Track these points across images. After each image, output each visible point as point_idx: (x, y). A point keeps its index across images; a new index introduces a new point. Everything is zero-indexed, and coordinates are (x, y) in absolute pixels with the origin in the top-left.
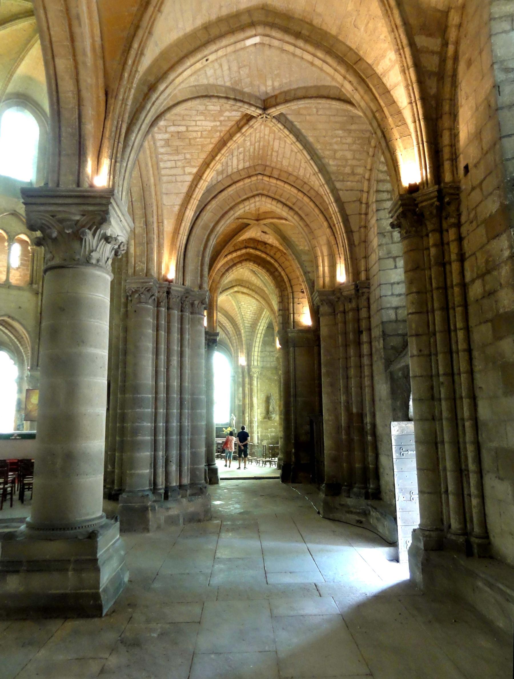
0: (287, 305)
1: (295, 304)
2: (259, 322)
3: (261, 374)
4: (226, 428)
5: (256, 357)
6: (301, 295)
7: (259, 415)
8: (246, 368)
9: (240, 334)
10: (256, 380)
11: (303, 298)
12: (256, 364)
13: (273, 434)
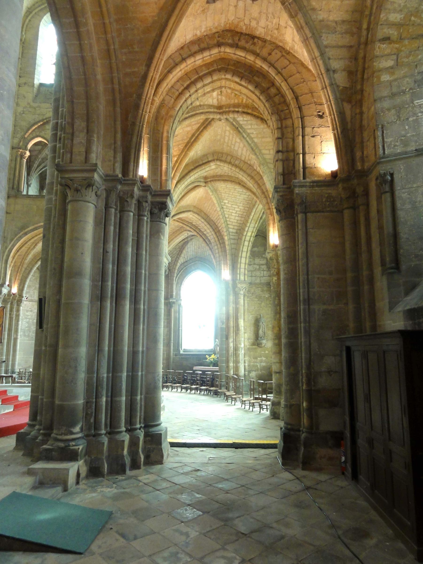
0: (291, 141)
1: (307, 138)
2: (246, 226)
3: (249, 291)
4: (210, 355)
5: (242, 270)
6: (318, 121)
7: (246, 340)
9: (224, 243)
10: (242, 298)
11: (320, 126)
12: (242, 278)
13: (264, 364)
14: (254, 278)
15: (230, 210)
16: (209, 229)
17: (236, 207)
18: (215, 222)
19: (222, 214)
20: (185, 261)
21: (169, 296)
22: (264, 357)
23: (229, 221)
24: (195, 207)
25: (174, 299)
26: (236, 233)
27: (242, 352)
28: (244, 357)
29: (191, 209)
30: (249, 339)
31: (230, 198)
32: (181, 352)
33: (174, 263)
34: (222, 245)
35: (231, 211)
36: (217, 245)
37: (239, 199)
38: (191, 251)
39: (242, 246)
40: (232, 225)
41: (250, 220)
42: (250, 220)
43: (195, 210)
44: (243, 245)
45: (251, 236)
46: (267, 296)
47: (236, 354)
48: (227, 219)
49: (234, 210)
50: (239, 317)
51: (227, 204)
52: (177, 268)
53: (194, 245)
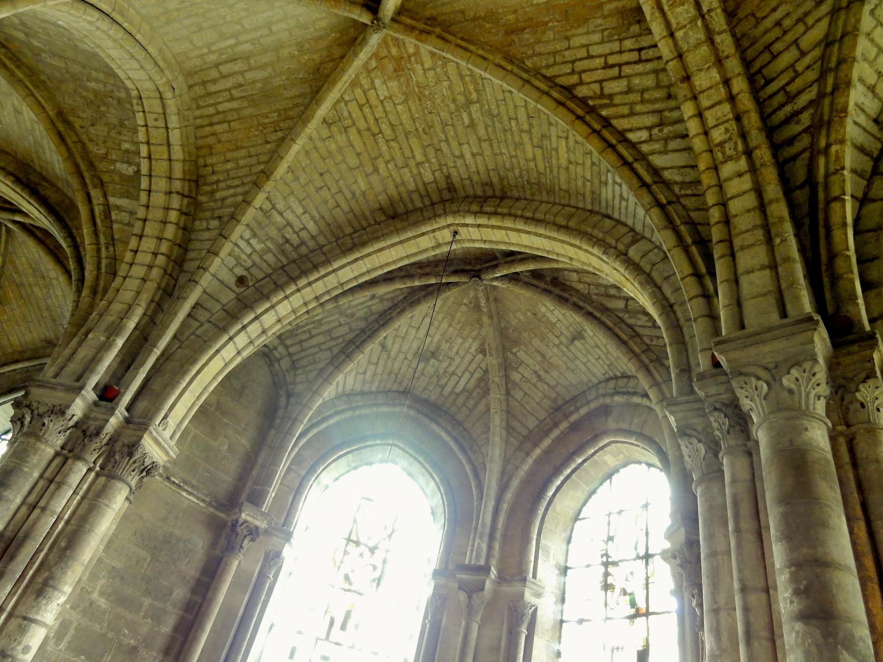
20: (358, 387)
25: (263, 514)
33: (322, 370)
38: (401, 356)
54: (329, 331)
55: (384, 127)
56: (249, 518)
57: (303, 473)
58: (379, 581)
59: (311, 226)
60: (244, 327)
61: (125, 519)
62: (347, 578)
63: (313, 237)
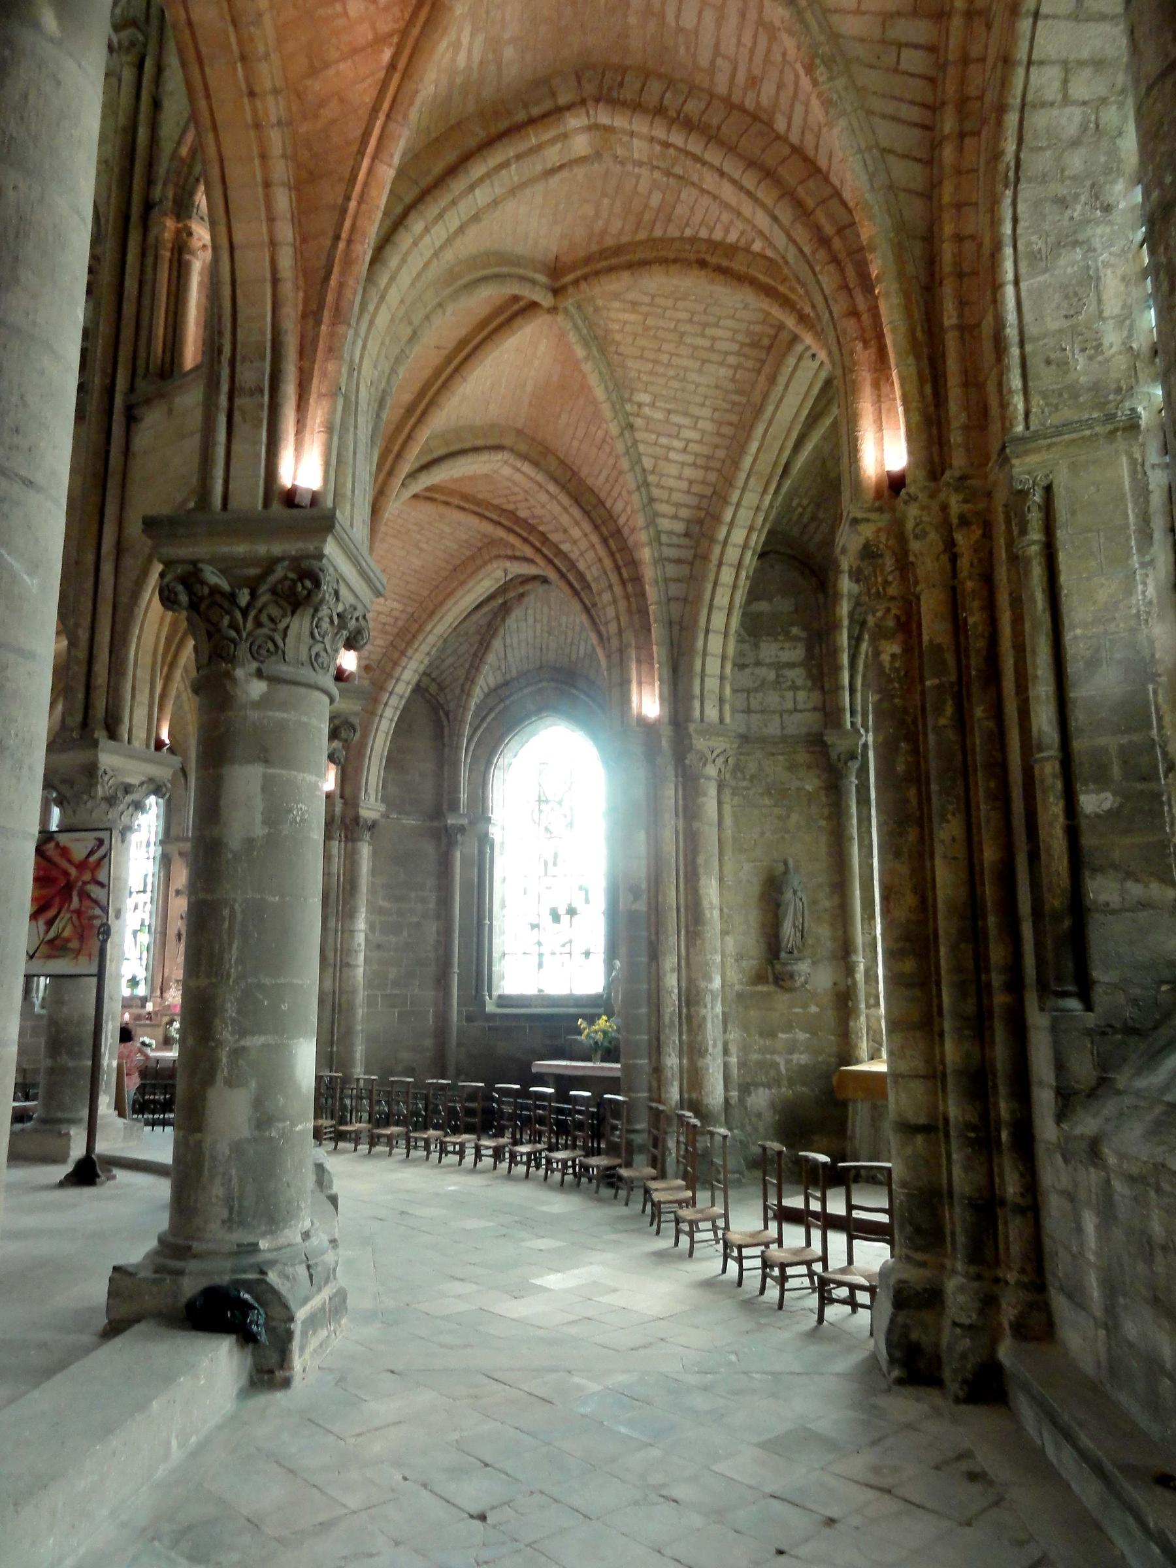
3: (738, 769)
4: (591, 1019)
5: (712, 684)
7: (730, 961)
8: (666, 732)
9: (637, 580)
10: (712, 791)
12: (712, 713)
13: (801, 1058)
14: (759, 716)
15: (659, 434)
16: (577, 523)
17: (686, 421)
18: (602, 495)
19: (627, 452)
20: (500, 680)
21: (445, 807)
22: (804, 1030)
23: (658, 486)
24: (520, 432)
25: (464, 815)
26: (687, 535)
27: (713, 1011)
28: (725, 1031)
29: (506, 442)
30: (739, 957)
31: (662, 381)
32: (490, 1008)
33: (463, 685)
34: (630, 588)
35: (663, 440)
36: (610, 587)
37: (698, 385)
38: (523, 645)
39: (709, 586)
40: (667, 502)
41: (742, 476)
42: (742, 476)
43: (523, 447)
44: (715, 584)
45: (745, 546)
46: (809, 788)
47: (689, 1018)
48: (651, 479)
49: (677, 437)
50: (701, 870)
51: (647, 410)
52: (473, 706)
53: (531, 621)
54: (455, 651)
55: (410, 526)
56: (454, 822)
57: (482, 768)
58: (571, 825)
59: (395, 605)
60: (386, 704)
61: (375, 854)
62: (547, 829)
63: (402, 612)
